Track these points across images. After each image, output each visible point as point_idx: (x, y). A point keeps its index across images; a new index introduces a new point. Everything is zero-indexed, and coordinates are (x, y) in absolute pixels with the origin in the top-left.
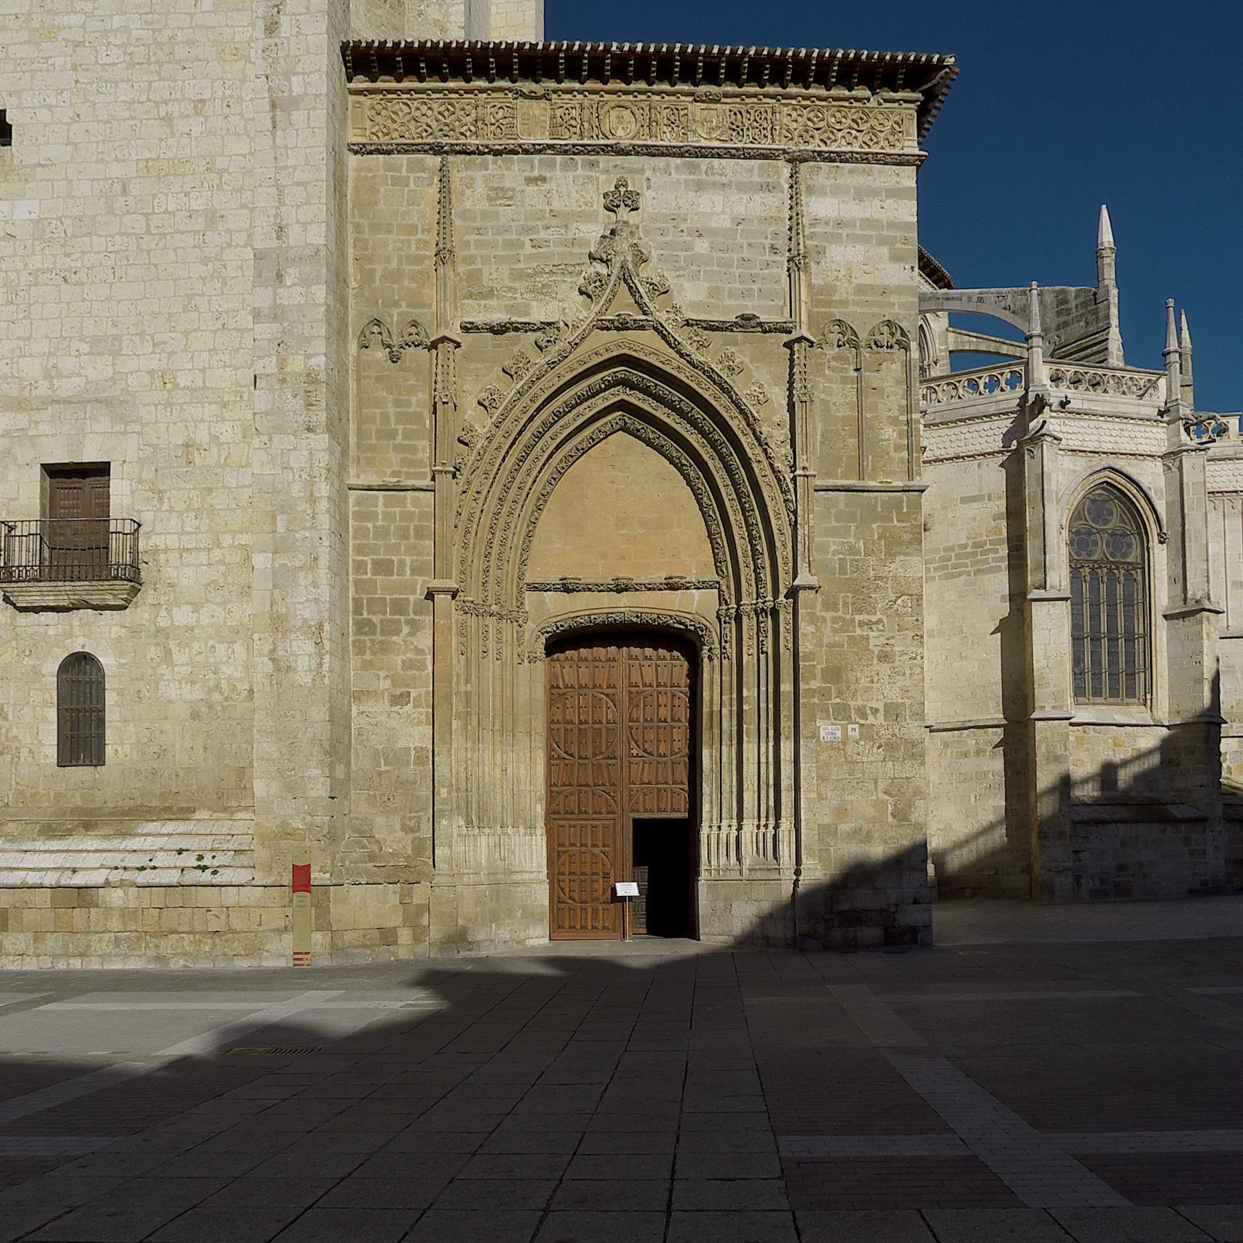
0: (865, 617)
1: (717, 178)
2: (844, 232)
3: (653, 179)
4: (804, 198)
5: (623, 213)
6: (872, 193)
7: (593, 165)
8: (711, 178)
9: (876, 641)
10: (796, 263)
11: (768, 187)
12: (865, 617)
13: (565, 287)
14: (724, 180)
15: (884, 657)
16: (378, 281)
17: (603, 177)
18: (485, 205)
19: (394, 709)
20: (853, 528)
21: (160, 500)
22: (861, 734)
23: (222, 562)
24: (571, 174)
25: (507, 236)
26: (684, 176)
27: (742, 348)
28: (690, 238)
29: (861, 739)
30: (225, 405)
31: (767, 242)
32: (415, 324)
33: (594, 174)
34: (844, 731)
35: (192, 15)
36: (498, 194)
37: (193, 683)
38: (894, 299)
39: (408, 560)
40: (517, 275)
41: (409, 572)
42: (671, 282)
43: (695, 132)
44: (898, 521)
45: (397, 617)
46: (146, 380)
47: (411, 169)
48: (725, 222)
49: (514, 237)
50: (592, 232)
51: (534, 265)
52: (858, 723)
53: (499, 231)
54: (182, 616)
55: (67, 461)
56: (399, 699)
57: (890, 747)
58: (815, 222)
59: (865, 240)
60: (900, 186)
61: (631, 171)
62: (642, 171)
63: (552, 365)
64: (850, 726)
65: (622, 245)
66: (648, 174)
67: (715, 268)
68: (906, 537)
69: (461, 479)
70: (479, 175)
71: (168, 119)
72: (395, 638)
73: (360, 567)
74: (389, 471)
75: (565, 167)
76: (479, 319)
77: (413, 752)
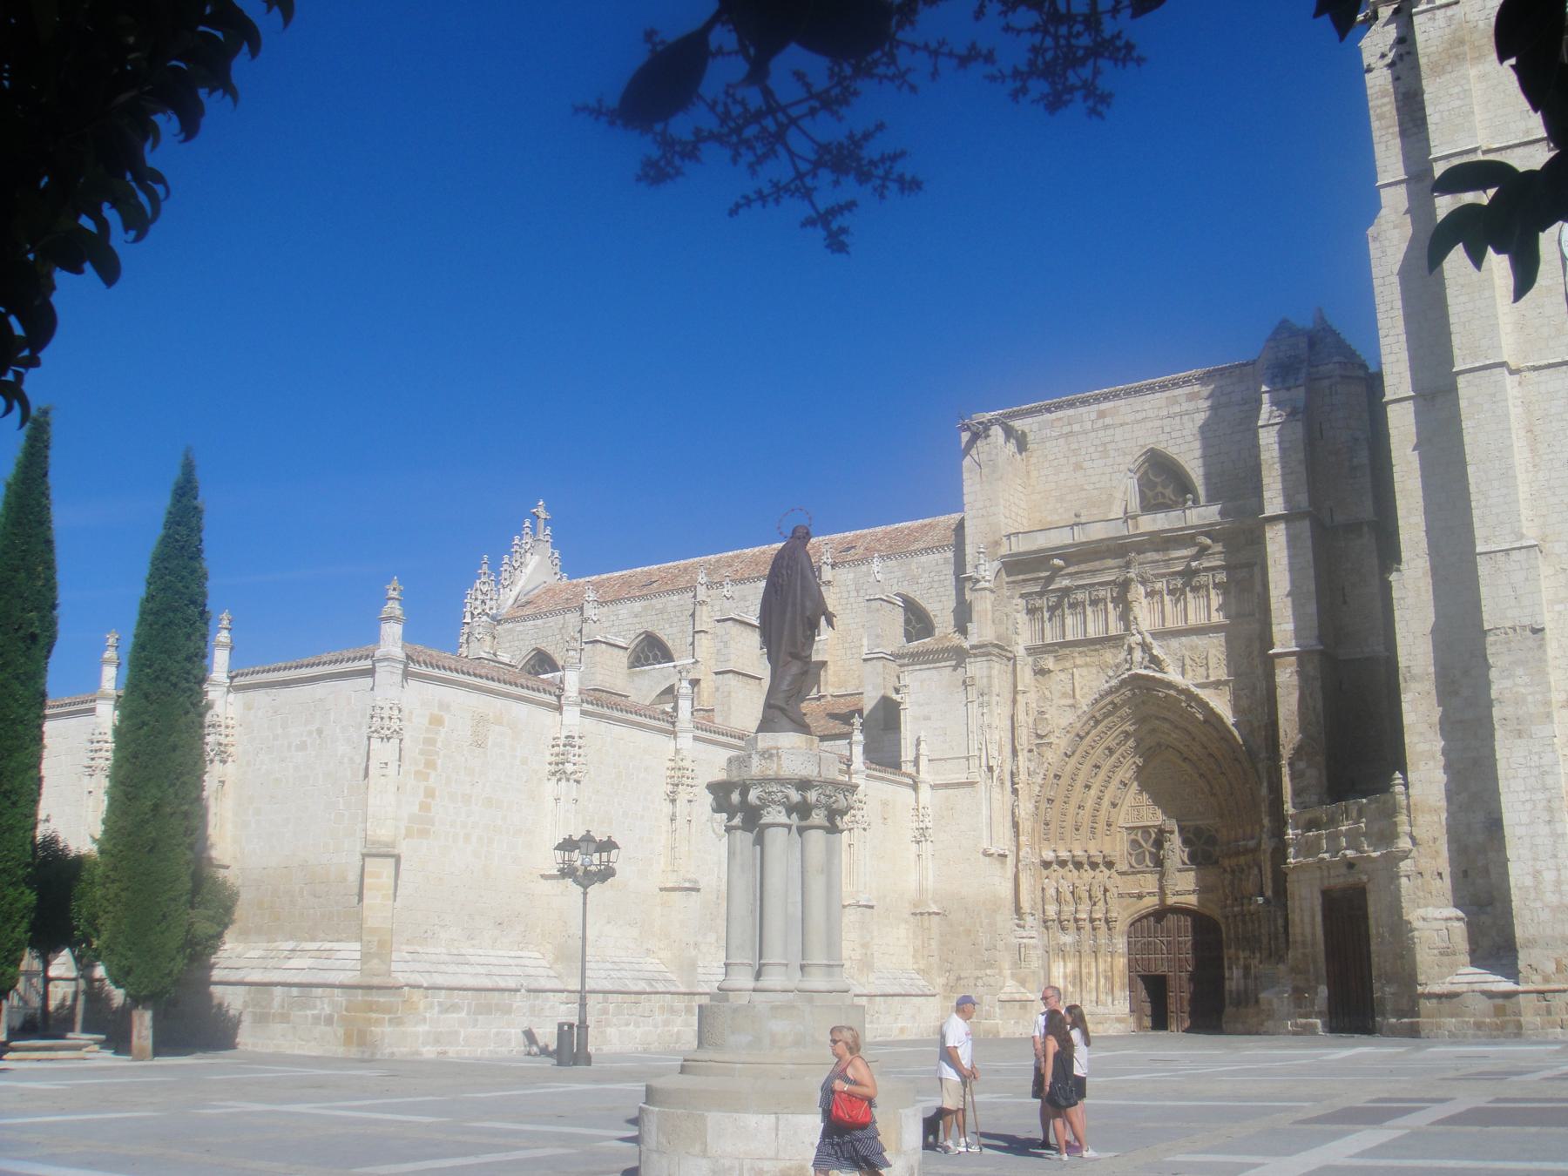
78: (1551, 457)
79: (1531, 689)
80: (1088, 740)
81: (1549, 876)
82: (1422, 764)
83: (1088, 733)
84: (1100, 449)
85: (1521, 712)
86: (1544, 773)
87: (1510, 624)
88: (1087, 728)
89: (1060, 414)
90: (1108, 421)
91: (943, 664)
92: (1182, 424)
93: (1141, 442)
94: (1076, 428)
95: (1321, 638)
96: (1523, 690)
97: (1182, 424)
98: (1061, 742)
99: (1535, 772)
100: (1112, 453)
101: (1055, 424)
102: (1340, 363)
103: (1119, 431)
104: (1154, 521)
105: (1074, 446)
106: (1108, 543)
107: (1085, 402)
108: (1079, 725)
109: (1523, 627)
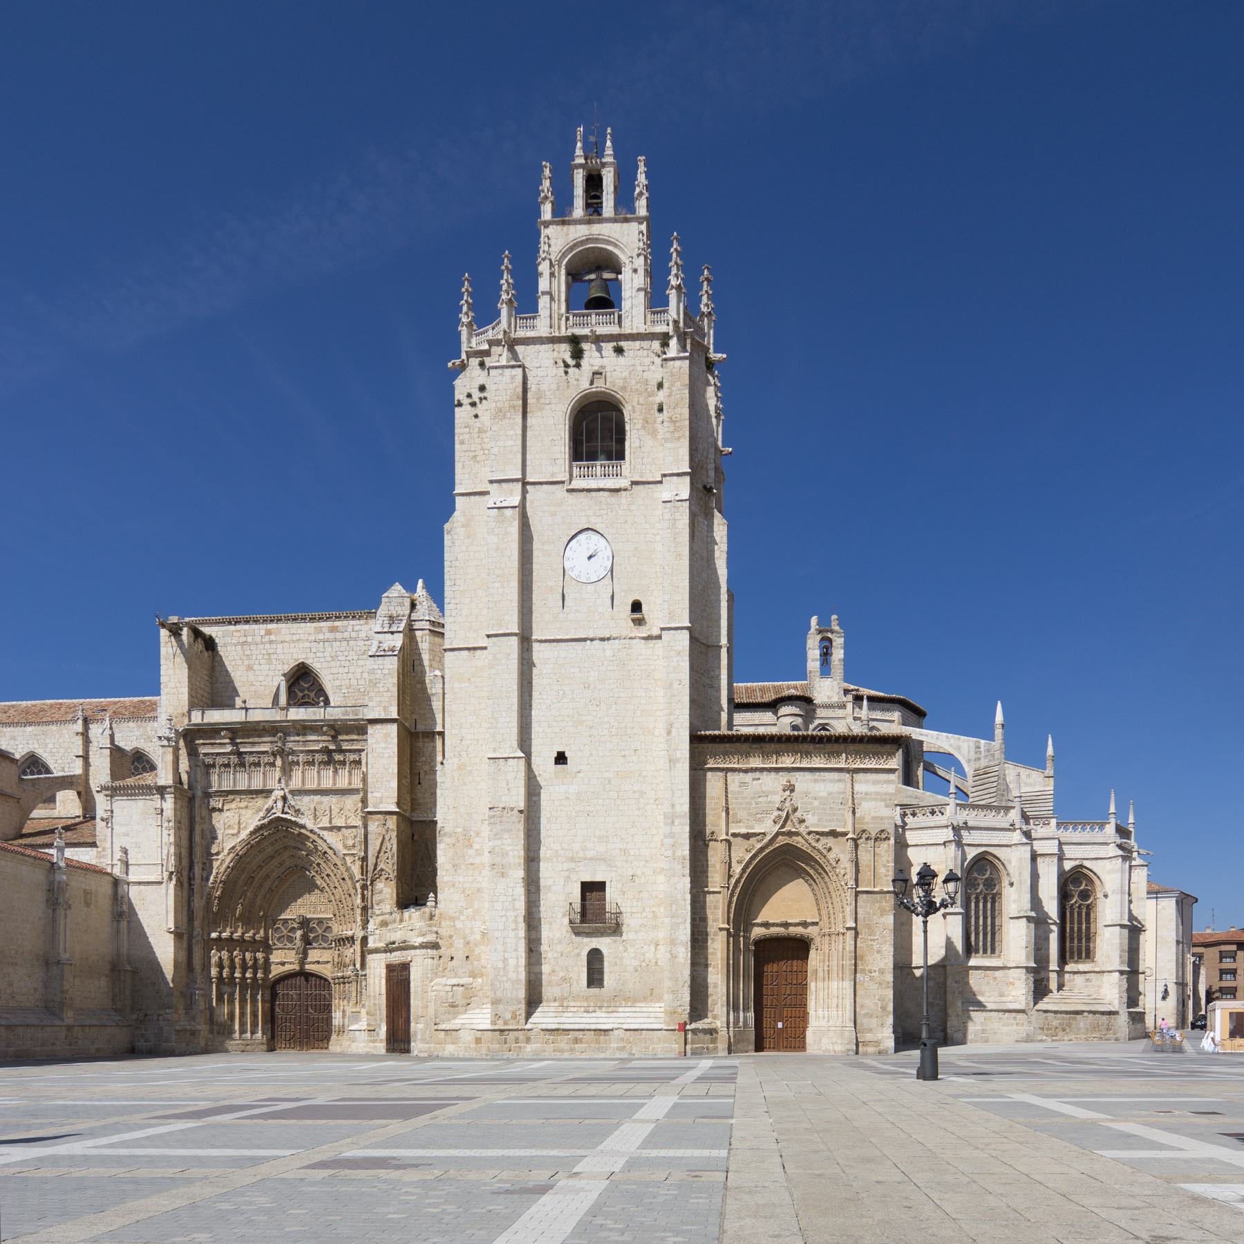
2: (869, 797)
5: (788, 793)
11: (839, 781)
23: (646, 917)
30: (647, 862)
31: (840, 801)
35: (633, 718)
36: (743, 784)
40: (750, 814)
46: (618, 852)
48: (824, 794)
50: (777, 799)
55: (589, 880)
65: (787, 804)
66: (797, 776)
75: (767, 775)
79: (512, 847)
81: (512, 962)
82: (446, 889)
84: (266, 657)
85: (504, 861)
86: (514, 900)
89: (239, 627)
90: (273, 637)
91: (140, 797)
92: (324, 648)
93: (295, 656)
94: (250, 639)
95: (398, 804)
96: (508, 848)
97: (324, 648)
99: (510, 899)
101: (235, 634)
102: (429, 621)
103: (280, 646)
104: (297, 713)
105: (247, 653)
106: (262, 724)
107: (256, 621)
109: (512, 809)
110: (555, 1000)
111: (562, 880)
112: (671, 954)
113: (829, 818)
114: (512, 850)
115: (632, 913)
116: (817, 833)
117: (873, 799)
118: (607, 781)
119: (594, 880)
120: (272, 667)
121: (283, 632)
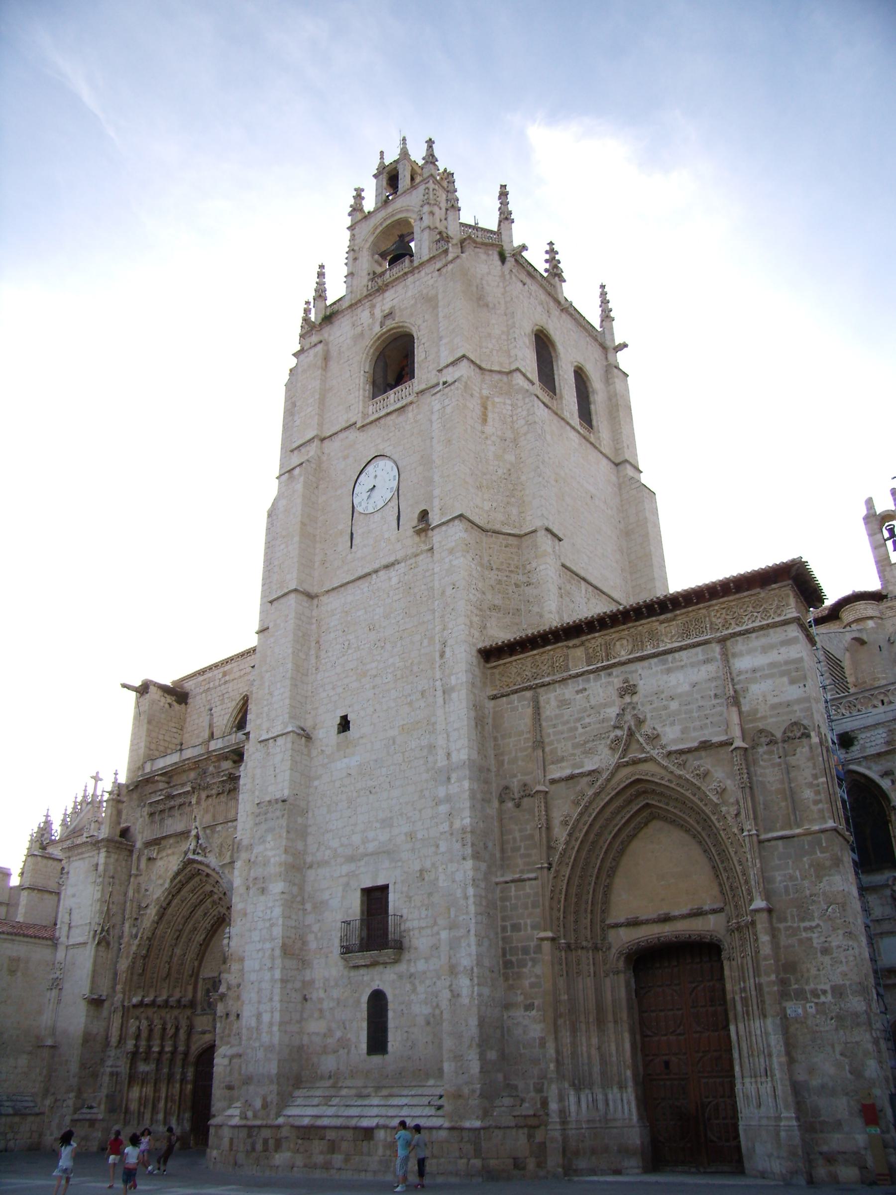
0: (807, 924)
1: (679, 664)
2: (758, 675)
3: (643, 675)
4: (731, 661)
5: (627, 699)
6: (772, 647)
7: (610, 675)
8: (675, 665)
9: (817, 942)
10: (735, 701)
11: (706, 661)
12: (807, 924)
13: (601, 747)
14: (683, 663)
15: (825, 951)
16: (506, 766)
17: (616, 680)
18: (557, 712)
19: (528, 1013)
20: (790, 863)
21: (410, 901)
22: (817, 1011)
24: (598, 683)
25: (569, 726)
26: (660, 668)
27: (705, 762)
28: (666, 703)
29: (817, 1014)
31: (712, 693)
32: (525, 785)
33: (610, 680)
34: (804, 1008)
37: (427, 1004)
38: (796, 708)
39: (529, 921)
40: (575, 746)
41: (529, 928)
42: (659, 730)
43: (663, 641)
44: (822, 852)
45: (525, 957)
47: (519, 702)
48: (686, 688)
49: (572, 725)
51: (584, 738)
52: (812, 1002)
53: (565, 723)
54: (421, 966)
56: (529, 1007)
57: (840, 1018)
58: (740, 673)
59: (772, 676)
60: (788, 638)
61: (631, 672)
62: (636, 671)
63: (597, 794)
64: (808, 1005)
65: (628, 717)
66: (640, 672)
67: (684, 716)
68: (828, 863)
69: (553, 870)
70: (552, 695)
71: (410, 704)
72: (524, 970)
73: (504, 929)
74: (518, 870)
75: (595, 680)
76: (556, 775)
77: (537, 1041)
78: (326, 660)
80: (170, 910)
81: (266, 1017)
83: (169, 904)
87: (268, 799)
88: (167, 901)
89: (205, 676)
93: (241, 691)
94: (211, 685)
96: (270, 853)
98: (152, 912)
99: (267, 925)
100: (226, 701)
103: (231, 685)
108: (162, 899)
109: (277, 801)
110: (330, 1077)
111: (341, 888)
112: (451, 991)
113: (697, 723)
114: (274, 856)
115: (421, 928)
116: (681, 752)
117: (765, 677)
118: (391, 742)
119: (375, 885)
120: (225, 706)
121: (235, 670)
